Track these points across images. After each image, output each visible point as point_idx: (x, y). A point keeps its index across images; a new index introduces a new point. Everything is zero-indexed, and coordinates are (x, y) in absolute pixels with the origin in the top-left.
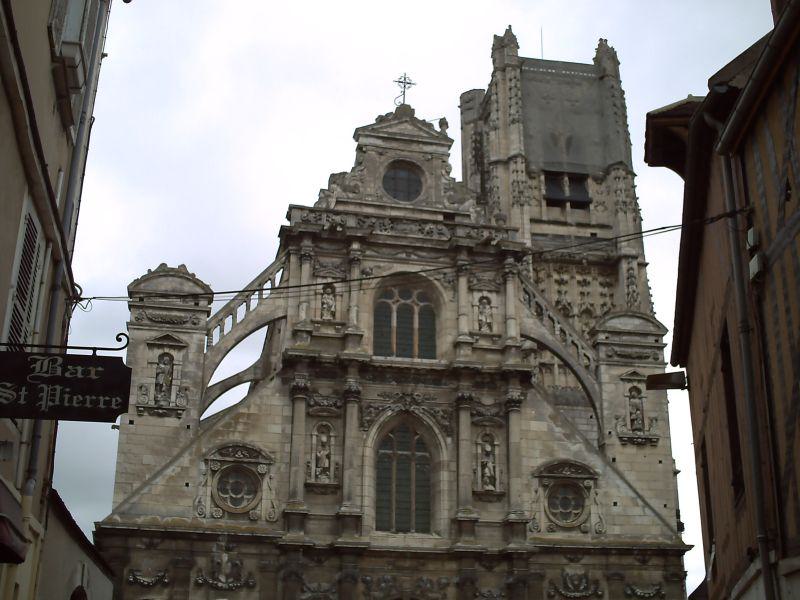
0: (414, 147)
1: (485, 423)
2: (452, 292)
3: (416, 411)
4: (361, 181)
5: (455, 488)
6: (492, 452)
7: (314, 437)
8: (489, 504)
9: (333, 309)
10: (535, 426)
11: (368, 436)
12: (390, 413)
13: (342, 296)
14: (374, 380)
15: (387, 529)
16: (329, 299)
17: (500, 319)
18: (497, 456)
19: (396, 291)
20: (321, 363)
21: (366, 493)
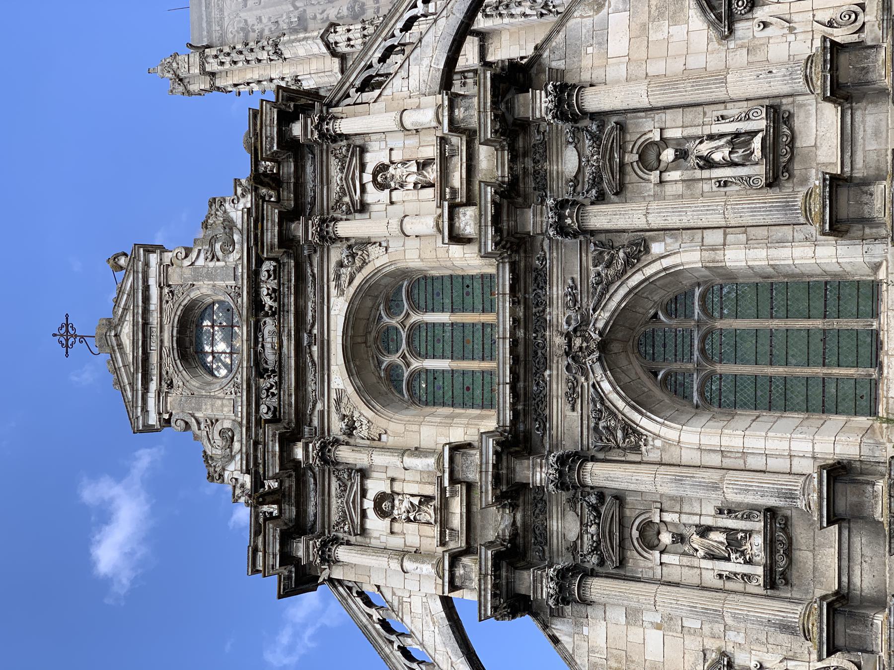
0: (154, 319)
1: (616, 168)
2: (370, 249)
3: (600, 325)
4: (213, 422)
5: (762, 232)
7: (666, 558)
8: (798, 144)
9: (416, 501)
10: (618, 45)
12: (606, 386)
13: (393, 480)
14: (544, 420)
16: (401, 507)
17: (412, 141)
18: (685, 134)
19: (387, 360)
20: (514, 536)
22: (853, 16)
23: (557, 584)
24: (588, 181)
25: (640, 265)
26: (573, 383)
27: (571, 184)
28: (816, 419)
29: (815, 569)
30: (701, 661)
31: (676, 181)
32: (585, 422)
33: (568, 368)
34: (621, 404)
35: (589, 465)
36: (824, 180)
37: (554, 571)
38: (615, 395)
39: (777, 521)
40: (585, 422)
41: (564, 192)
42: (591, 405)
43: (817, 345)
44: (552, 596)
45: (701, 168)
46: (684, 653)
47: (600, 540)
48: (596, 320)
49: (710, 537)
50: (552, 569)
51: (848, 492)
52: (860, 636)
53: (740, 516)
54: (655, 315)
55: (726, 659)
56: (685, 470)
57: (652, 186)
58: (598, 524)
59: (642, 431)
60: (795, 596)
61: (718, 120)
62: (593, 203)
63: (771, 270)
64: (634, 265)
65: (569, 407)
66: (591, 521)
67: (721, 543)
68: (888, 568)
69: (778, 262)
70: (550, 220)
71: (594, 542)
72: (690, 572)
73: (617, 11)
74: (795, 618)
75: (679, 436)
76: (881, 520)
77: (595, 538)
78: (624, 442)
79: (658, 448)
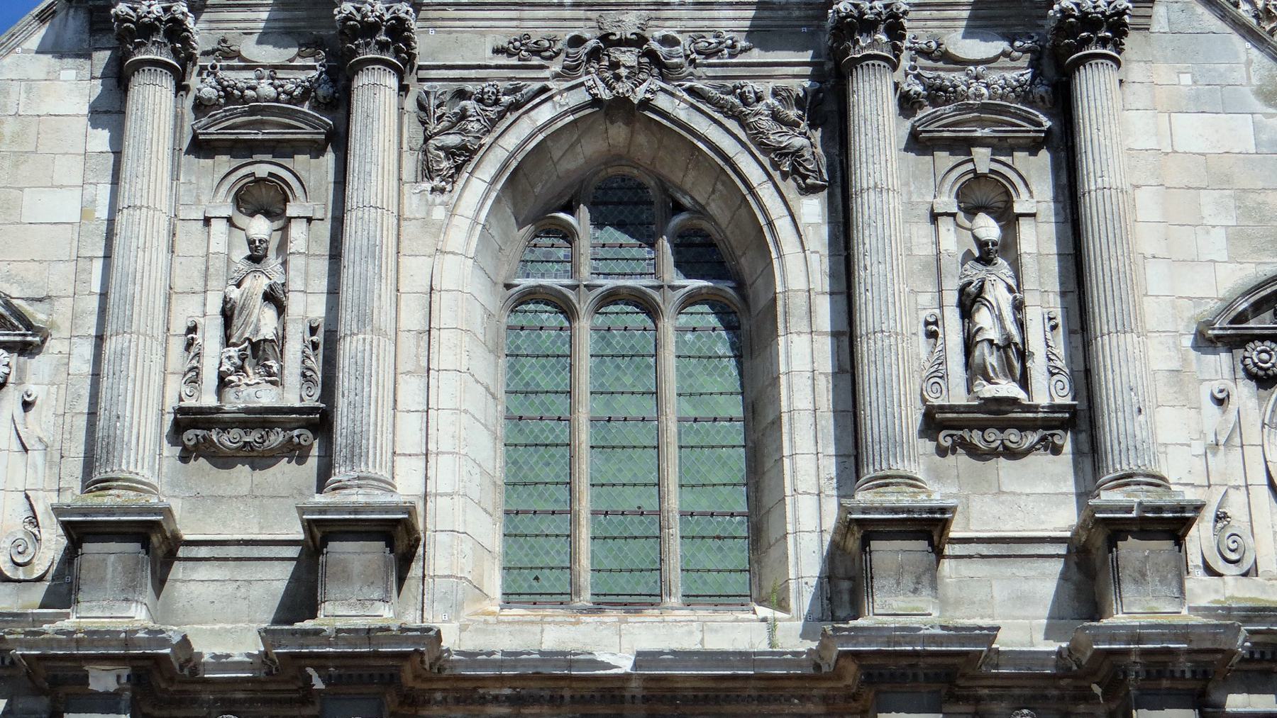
3: (662, 101)
6: (1008, 247)
7: (219, 227)
8: (1002, 461)
11: (452, 213)
12: (544, 113)
15: (563, 598)
18: (1025, 260)
21: (445, 429)
22: (1233, 557)
23: (158, 19)
24: (939, 77)
25: (777, 175)
26: (546, 50)
27: (933, 45)
28: (495, 499)
29: (218, 499)
30: (29, 293)
31: (937, 243)
32: (473, 74)
33: (577, 41)
34: (511, 141)
35: (392, 81)
36: (943, 510)
37: (183, 13)
38: (527, 132)
39: (303, 431)
40: (473, 74)
41: (917, 32)
42: (507, 85)
43: (630, 499)
44: (134, 10)
45: (962, 291)
46: (40, 262)
47: (245, 102)
48: (672, 95)
49: (266, 309)
50: (186, 10)
51: (370, 556)
52: (103, 579)
53: (308, 363)
54: (678, 208)
55: (37, 339)
56: (392, 264)
57: (930, 199)
58: (277, 100)
59: (461, 182)
60: (165, 463)
61: (1050, 319)
62: (896, 85)
63: (771, 418)
64: (776, 166)
65: (503, 42)
66: (282, 86)
67: (257, 331)
68: (229, 626)
69: (785, 429)
70: (868, 5)
71: (242, 92)
72: (196, 274)
73: (1257, 129)
74: (128, 463)
75: (453, 253)
76: (321, 614)
77: (249, 93)
78: (438, 148)
79: (429, 213)
